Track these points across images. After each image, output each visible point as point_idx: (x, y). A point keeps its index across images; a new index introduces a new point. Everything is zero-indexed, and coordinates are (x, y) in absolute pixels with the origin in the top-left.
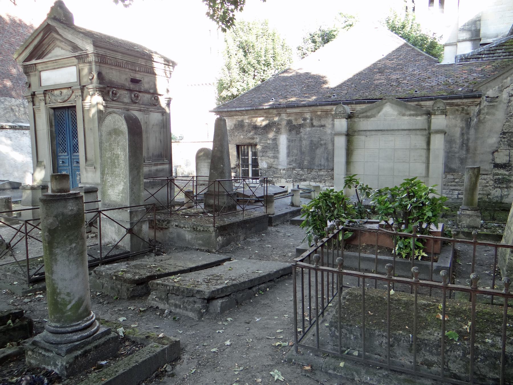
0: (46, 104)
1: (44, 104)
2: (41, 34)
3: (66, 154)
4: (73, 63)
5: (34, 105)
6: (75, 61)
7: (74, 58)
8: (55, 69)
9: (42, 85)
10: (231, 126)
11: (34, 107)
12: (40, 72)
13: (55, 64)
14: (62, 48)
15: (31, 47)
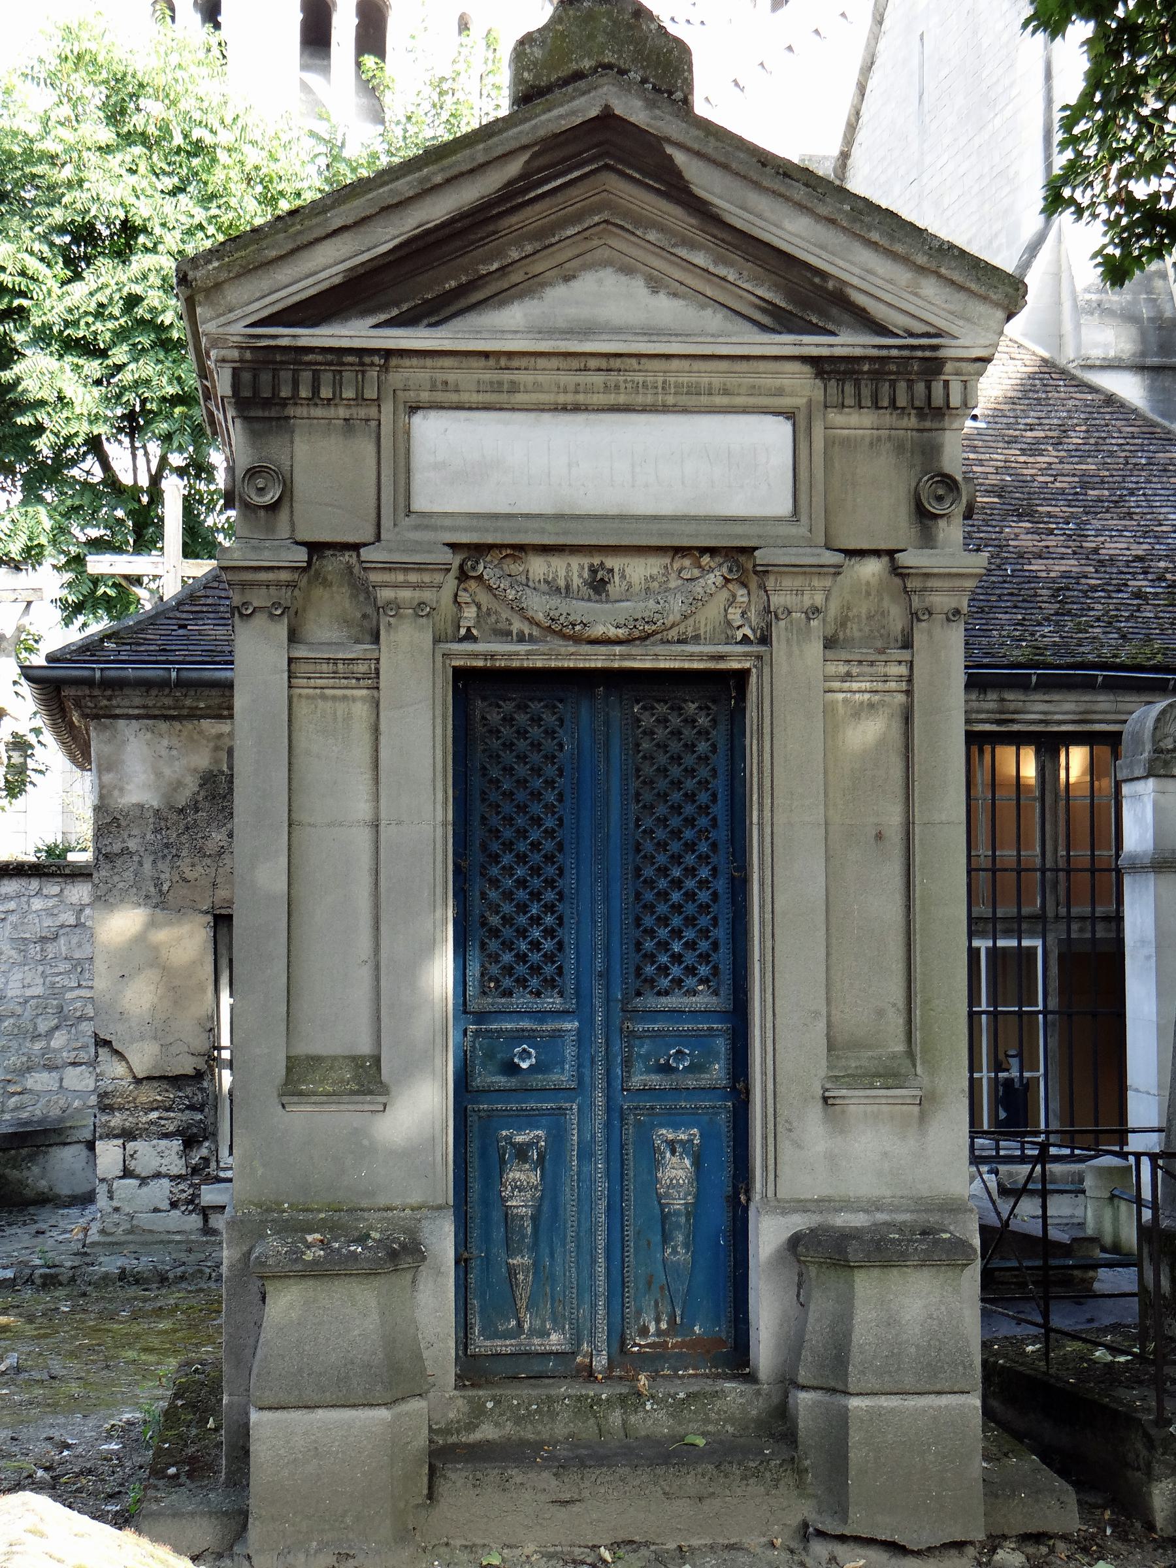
0: (437, 640)
1: (429, 637)
2: (514, 168)
3: (552, 1002)
4: (780, 392)
5: (293, 637)
6: (801, 386)
7: (796, 367)
8: (577, 408)
9: (420, 504)
10: (178, 785)
11: (301, 652)
12: (414, 409)
13: (598, 379)
14: (655, 284)
15: (386, 237)
